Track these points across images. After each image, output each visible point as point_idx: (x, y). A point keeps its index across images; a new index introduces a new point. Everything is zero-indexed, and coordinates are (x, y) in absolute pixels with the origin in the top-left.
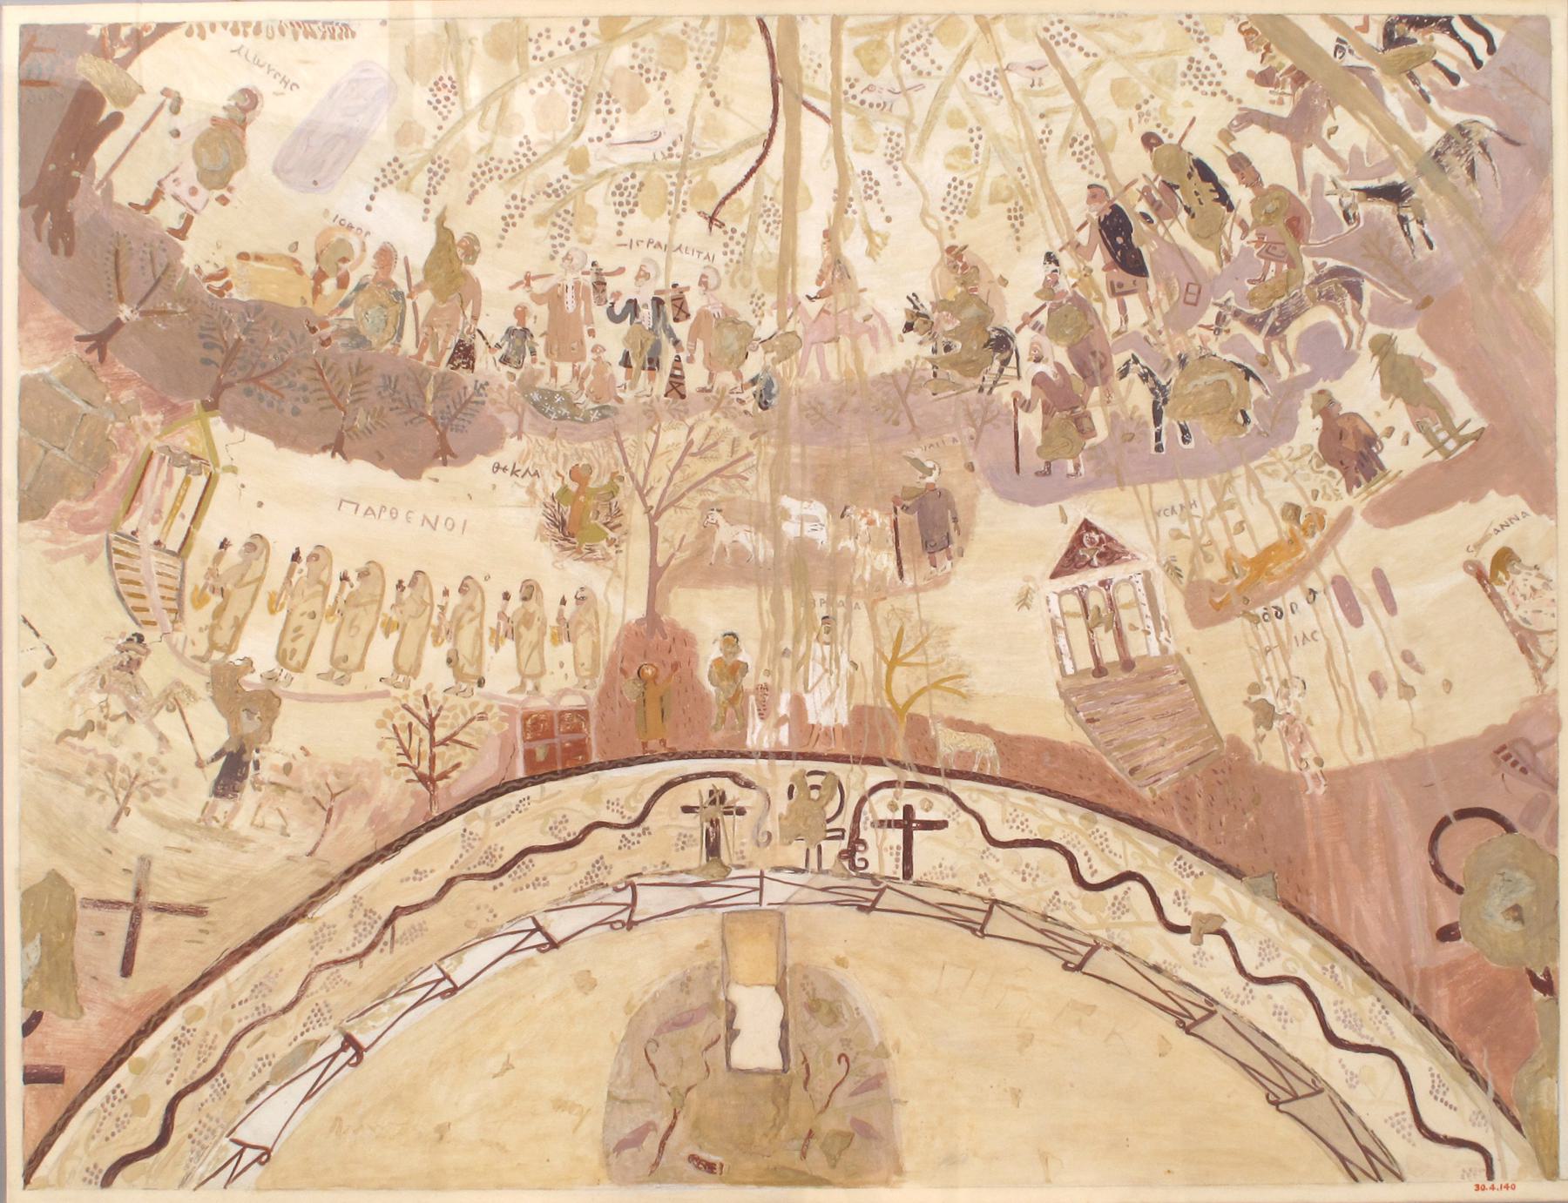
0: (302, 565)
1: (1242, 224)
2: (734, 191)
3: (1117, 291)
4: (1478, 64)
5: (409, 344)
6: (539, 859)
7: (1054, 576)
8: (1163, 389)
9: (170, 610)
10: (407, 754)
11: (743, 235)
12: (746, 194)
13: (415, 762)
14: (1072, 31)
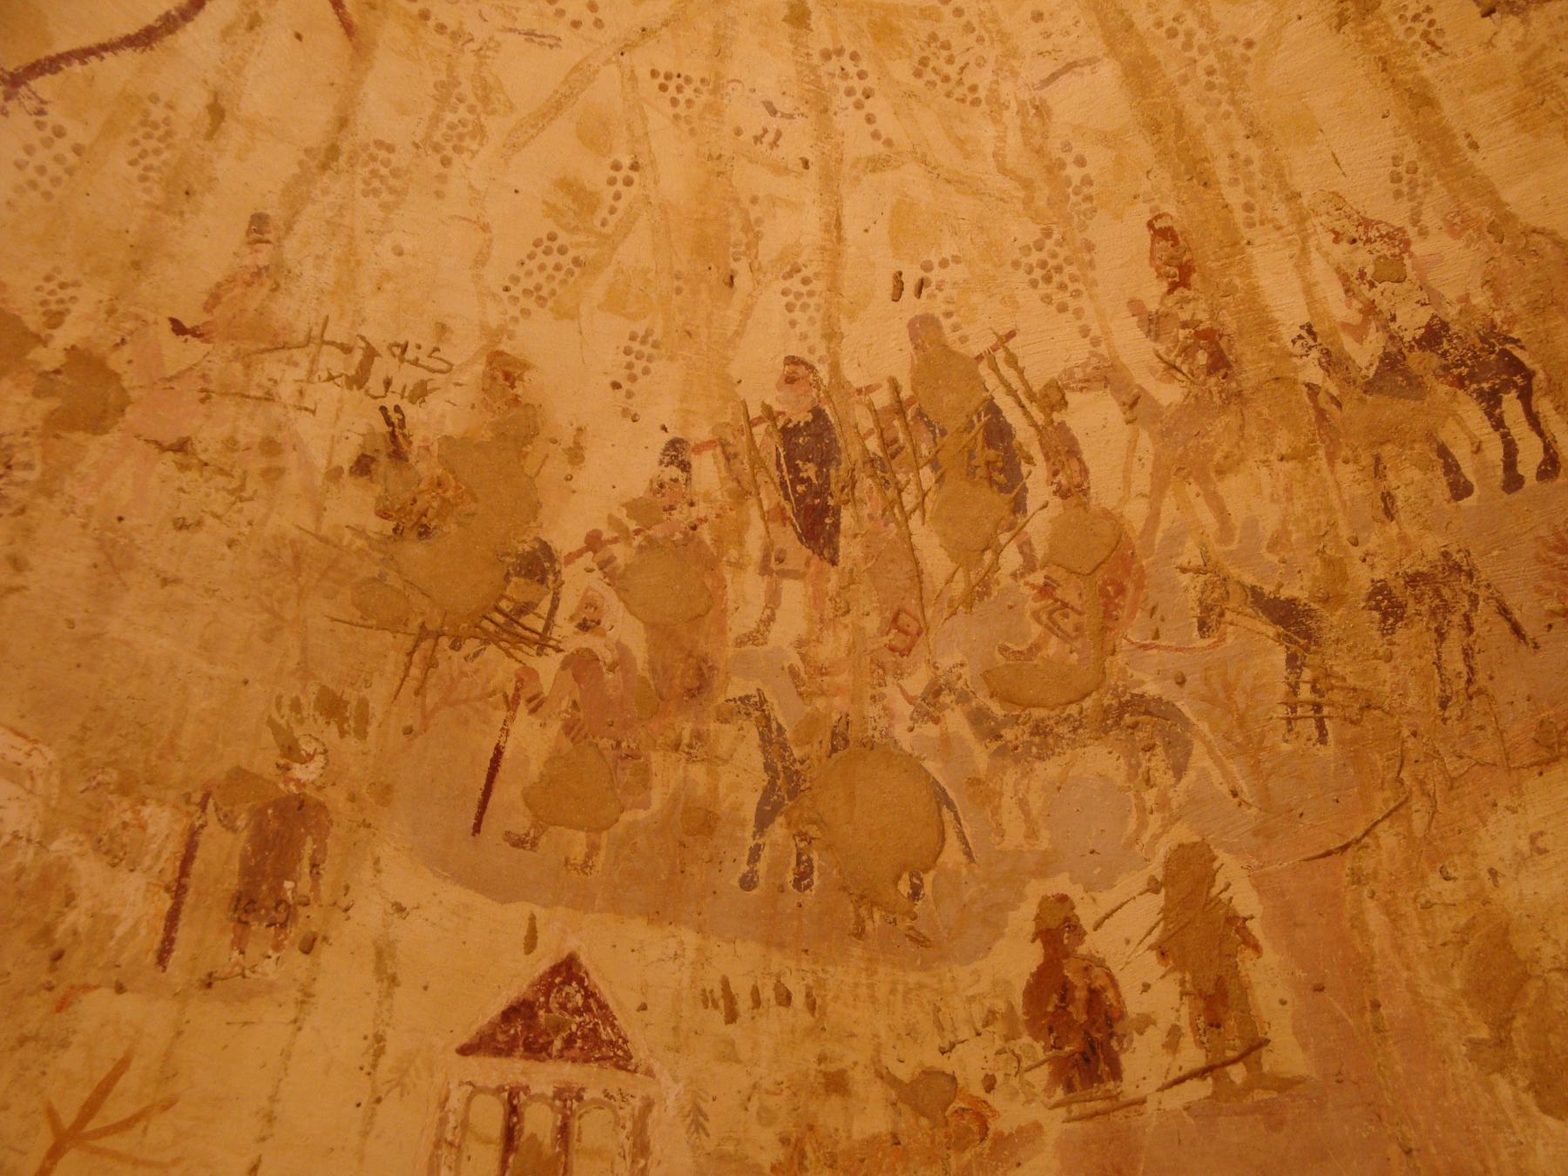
1: (1025, 548)
2: (84, 54)
3: (769, 563)
4: (1513, 481)
7: (464, 1051)
8: (793, 778)
11: (78, 150)
12: (118, 69)
14: (867, 83)
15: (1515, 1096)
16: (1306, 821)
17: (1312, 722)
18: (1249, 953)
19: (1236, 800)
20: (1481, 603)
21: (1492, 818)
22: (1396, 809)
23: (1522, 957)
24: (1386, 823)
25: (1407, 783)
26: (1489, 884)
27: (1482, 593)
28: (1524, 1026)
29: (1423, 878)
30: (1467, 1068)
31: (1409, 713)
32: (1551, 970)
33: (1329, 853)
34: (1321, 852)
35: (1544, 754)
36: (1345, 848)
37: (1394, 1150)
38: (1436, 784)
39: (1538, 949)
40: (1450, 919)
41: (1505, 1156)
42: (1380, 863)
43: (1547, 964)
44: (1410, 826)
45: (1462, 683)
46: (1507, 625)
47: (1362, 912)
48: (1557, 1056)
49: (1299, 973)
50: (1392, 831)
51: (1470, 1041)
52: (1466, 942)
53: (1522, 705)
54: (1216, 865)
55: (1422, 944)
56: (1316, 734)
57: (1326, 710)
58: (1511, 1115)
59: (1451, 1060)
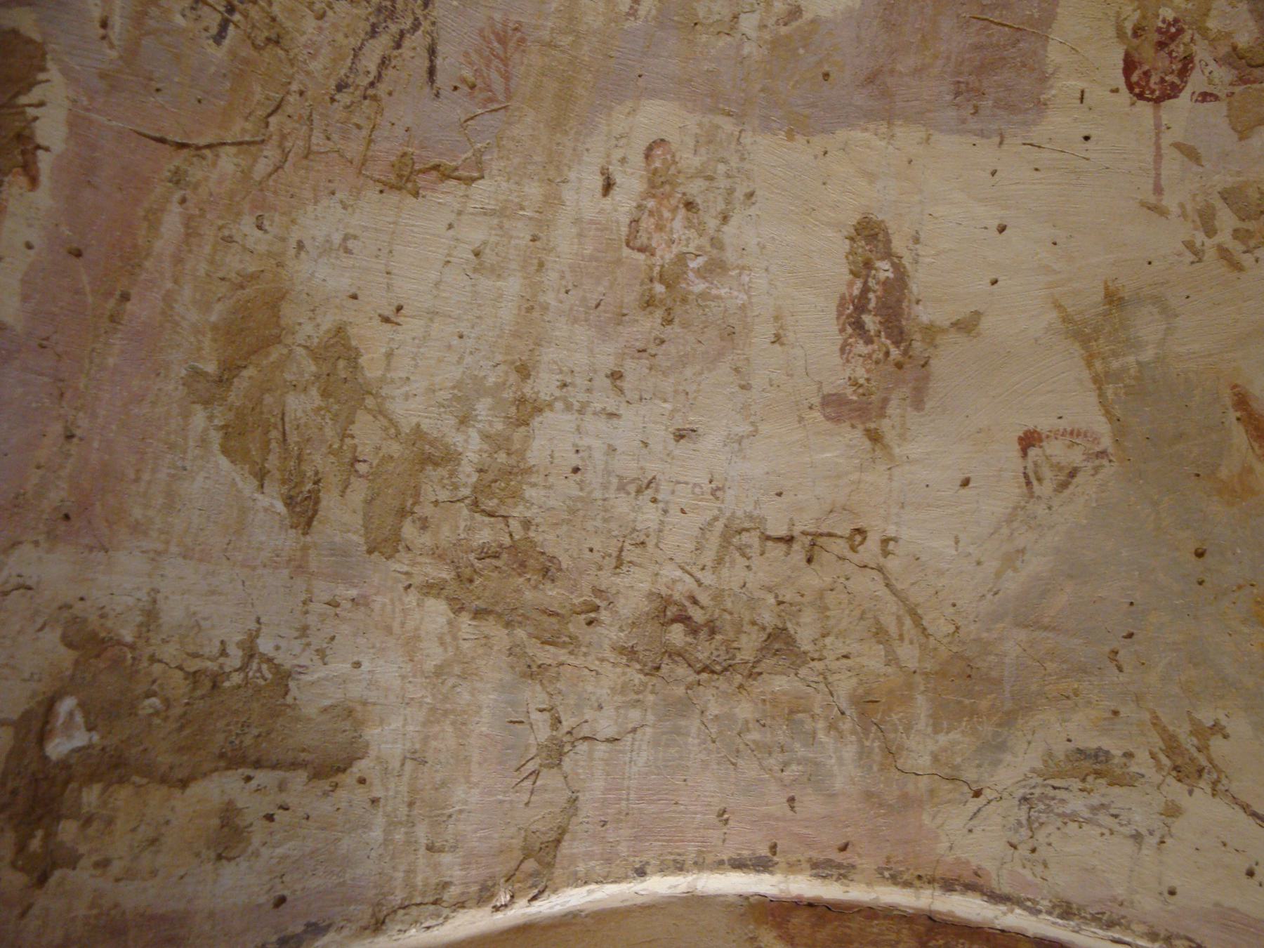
15: (205, 430)
16: (160, 99)
17: (218, 18)
18: (23, 180)
19: (102, 32)
20: (419, 33)
21: (325, 202)
22: (249, 143)
23: (283, 323)
24: (233, 150)
25: (271, 128)
26: (292, 252)
27: (426, 25)
28: (250, 378)
29: (239, 214)
30: (176, 389)
31: (308, 73)
32: (299, 345)
33: (162, 141)
34: (158, 135)
35: (393, 178)
36: (183, 146)
37: (57, 428)
38: (296, 145)
39: (300, 324)
40: (241, 261)
41: (162, 475)
42: (206, 179)
43: (300, 338)
44: (253, 165)
45: (366, 81)
46: (427, 64)
47: (163, 210)
48: (262, 413)
49: (65, 230)
50: (235, 160)
51: (193, 368)
52: (242, 287)
53: (400, 131)
54: (41, 76)
55: (203, 268)
56: (214, 30)
57: (237, 17)
58: (191, 443)
59: (166, 376)
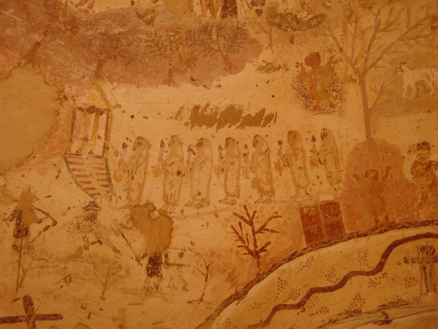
0: (167, 148)
5: (197, 9)
6: (321, 295)
9: (104, 186)
10: (241, 239)
13: (247, 244)
